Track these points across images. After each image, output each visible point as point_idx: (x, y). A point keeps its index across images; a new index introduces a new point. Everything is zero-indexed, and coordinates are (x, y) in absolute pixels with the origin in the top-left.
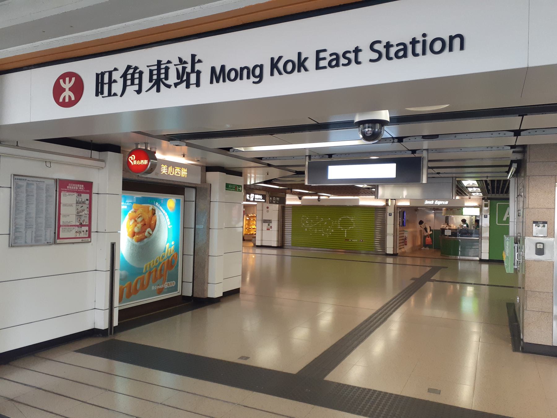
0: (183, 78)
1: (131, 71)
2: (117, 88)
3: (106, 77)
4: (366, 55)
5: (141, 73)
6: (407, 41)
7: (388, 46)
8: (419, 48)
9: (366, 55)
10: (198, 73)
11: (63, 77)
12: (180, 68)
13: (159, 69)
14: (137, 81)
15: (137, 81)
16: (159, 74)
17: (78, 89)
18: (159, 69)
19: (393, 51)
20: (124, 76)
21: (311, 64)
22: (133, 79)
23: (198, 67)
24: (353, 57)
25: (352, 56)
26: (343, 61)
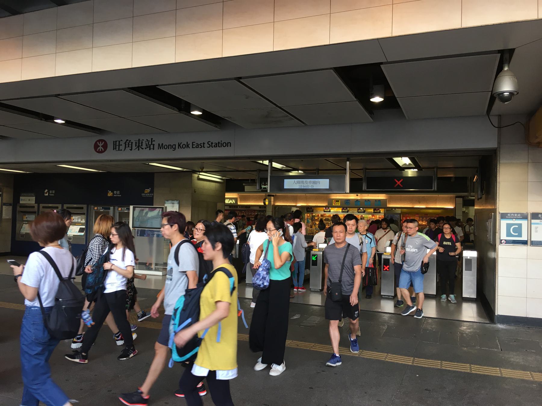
0: (148, 147)
1: (128, 142)
2: (122, 147)
3: (118, 143)
4: (206, 145)
5: (132, 143)
7: (212, 143)
9: (206, 145)
10: (154, 145)
11: (99, 141)
12: (147, 143)
13: (139, 142)
14: (130, 146)
15: (130, 146)
16: (139, 144)
17: (105, 147)
18: (139, 142)
19: (213, 145)
20: (125, 143)
21: (190, 146)
22: (129, 145)
23: (153, 143)
24: (202, 146)
25: (202, 145)
26: (200, 146)
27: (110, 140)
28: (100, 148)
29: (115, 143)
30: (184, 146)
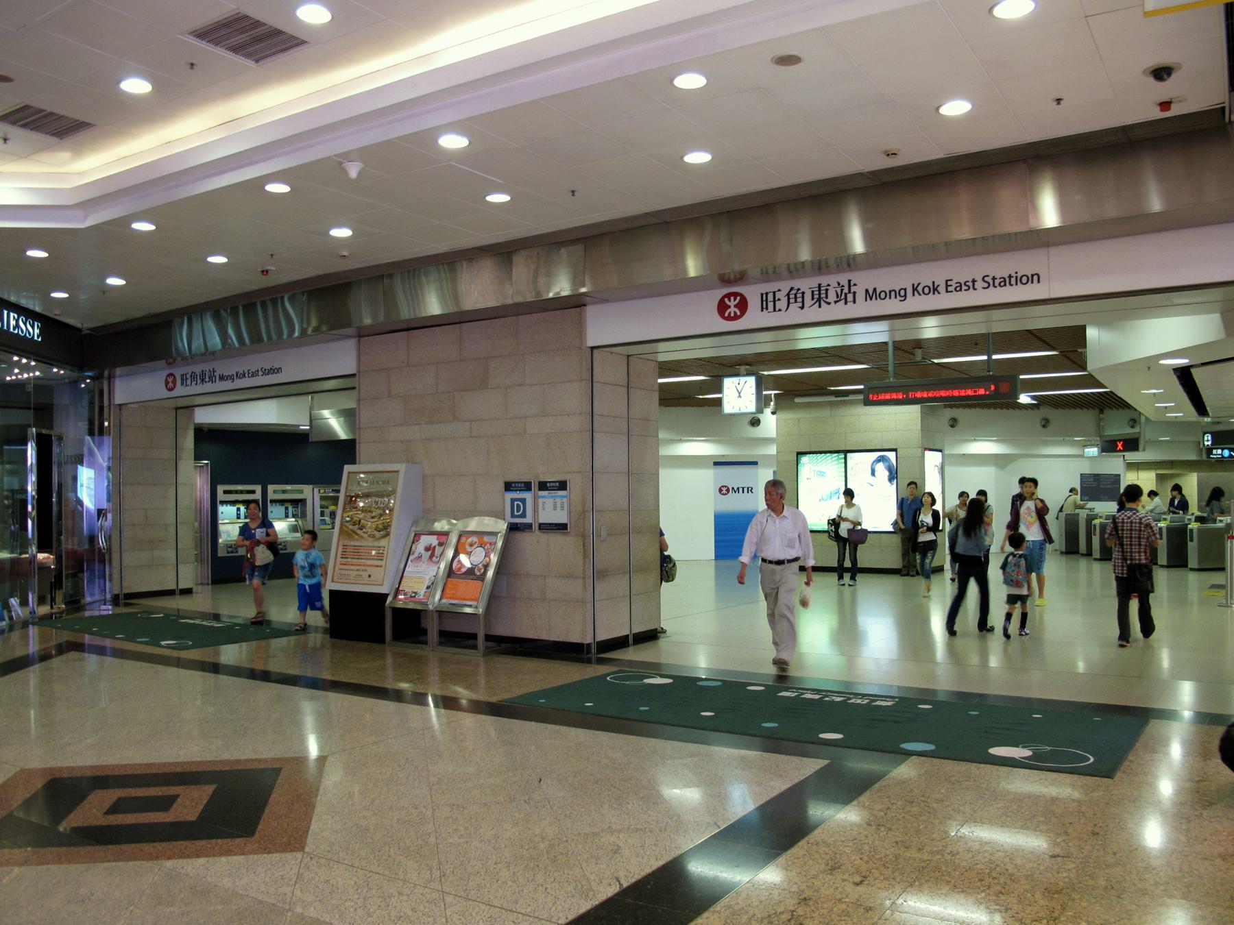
2: (782, 304)
6: (1006, 276)
7: (994, 279)
8: (1013, 280)
11: (728, 296)
12: (839, 290)
14: (799, 300)
15: (799, 300)
17: (743, 306)
19: (997, 282)
20: (788, 295)
21: (942, 289)
22: (796, 298)
23: (853, 289)
24: (971, 285)
25: (970, 284)
26: (964, 287)
27: (752, 293)
28: (733, 310)
29: (764, 298)
30: (926, 290)
